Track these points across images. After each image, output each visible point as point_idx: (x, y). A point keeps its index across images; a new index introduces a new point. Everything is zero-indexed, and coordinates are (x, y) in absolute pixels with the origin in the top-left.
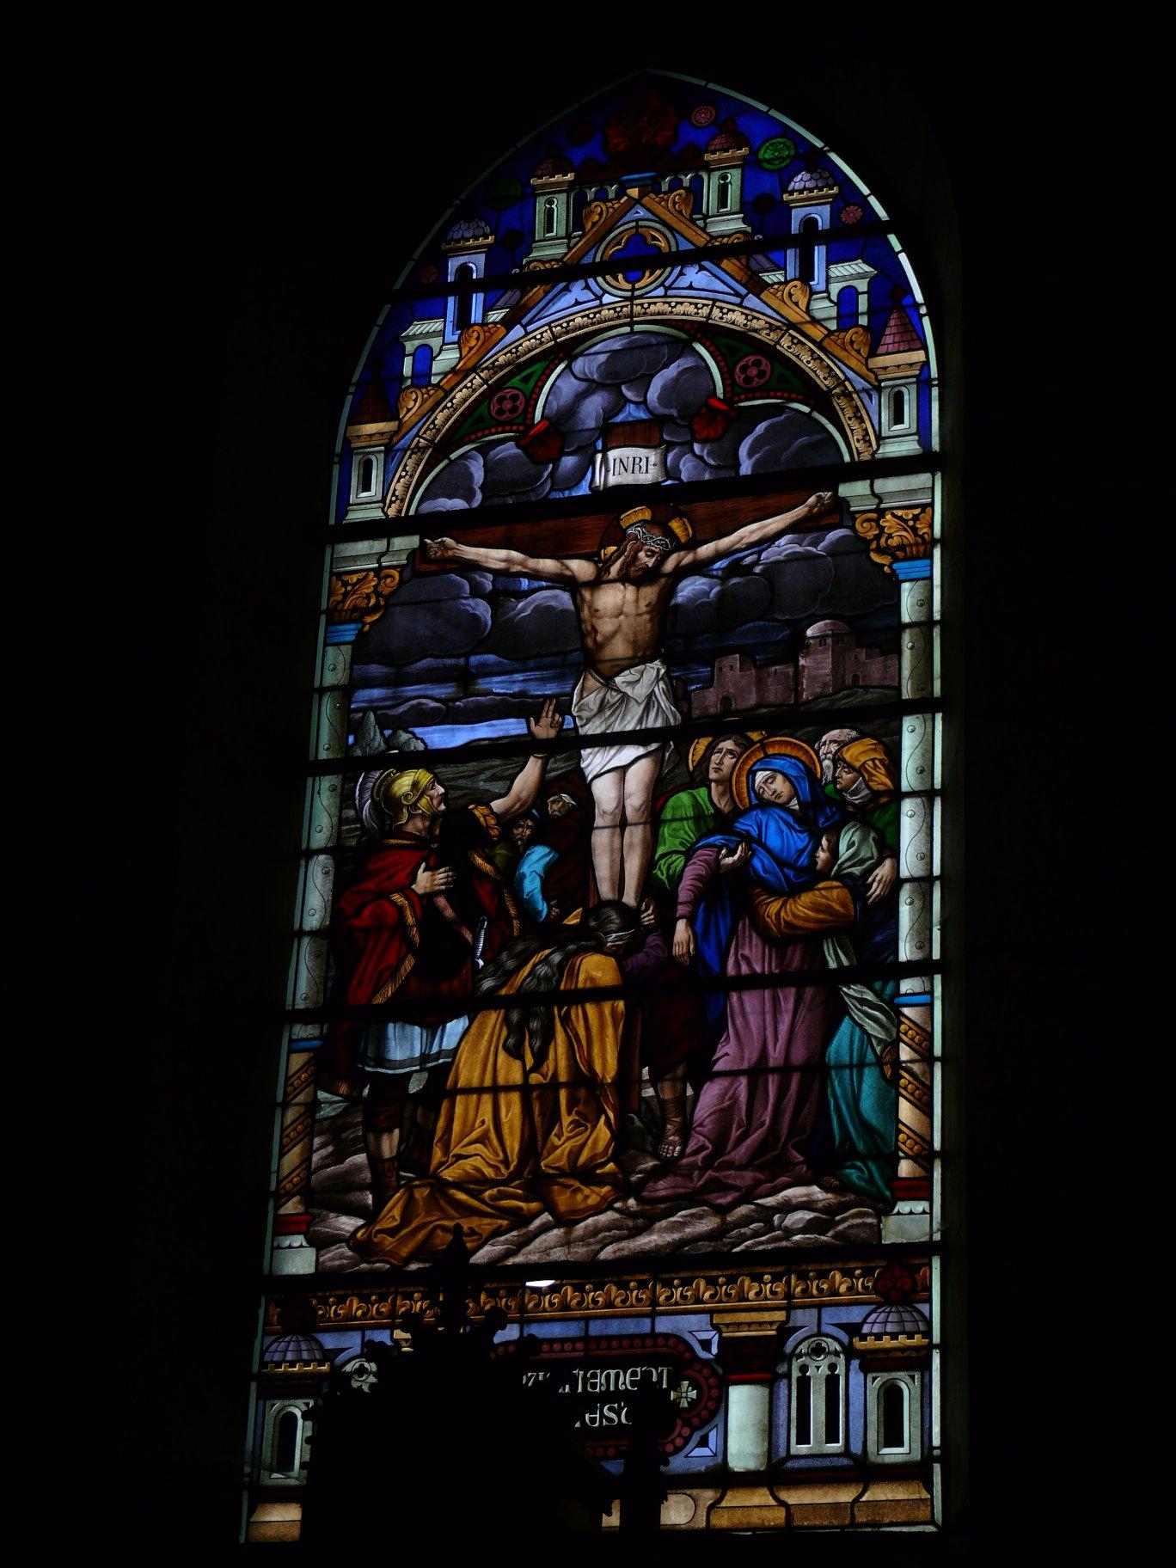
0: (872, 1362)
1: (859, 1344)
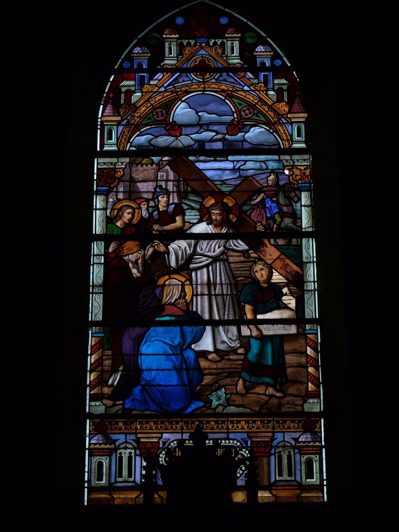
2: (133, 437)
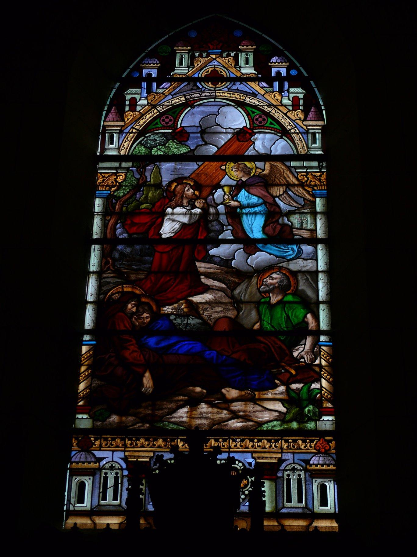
0: (314, 474)
2: (121, 455)
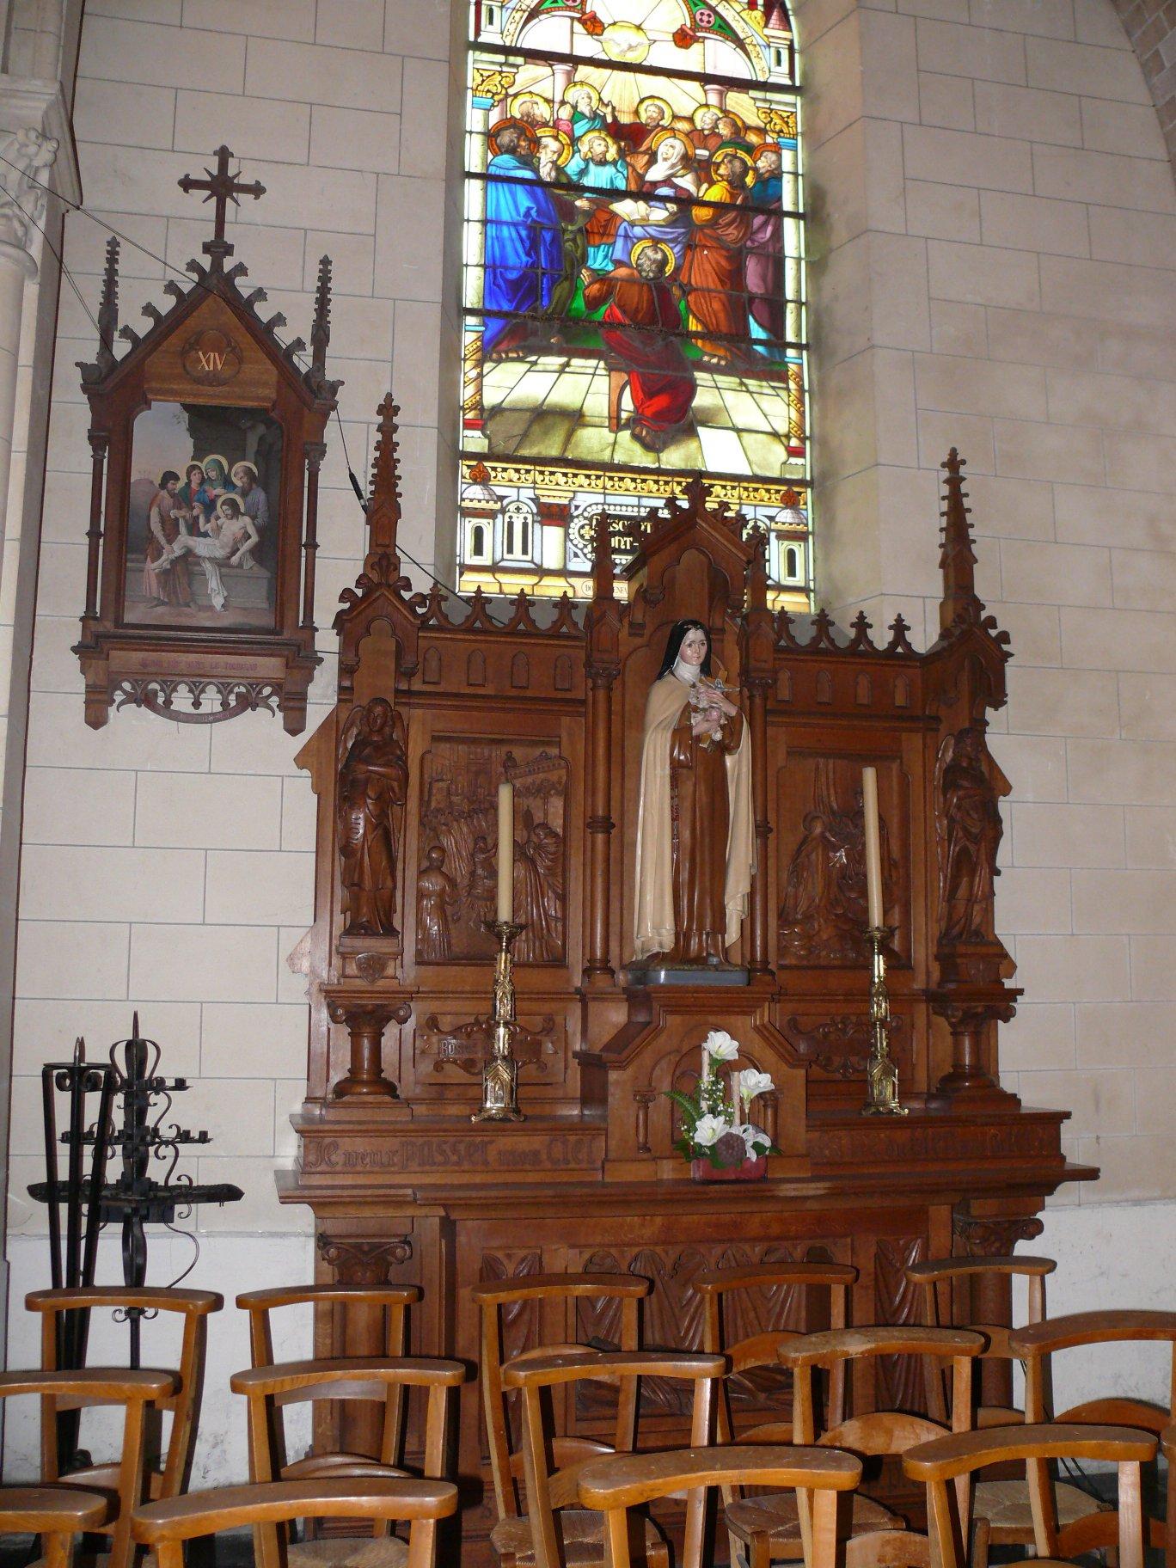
0: (782, 536)
1: (773, 526)
